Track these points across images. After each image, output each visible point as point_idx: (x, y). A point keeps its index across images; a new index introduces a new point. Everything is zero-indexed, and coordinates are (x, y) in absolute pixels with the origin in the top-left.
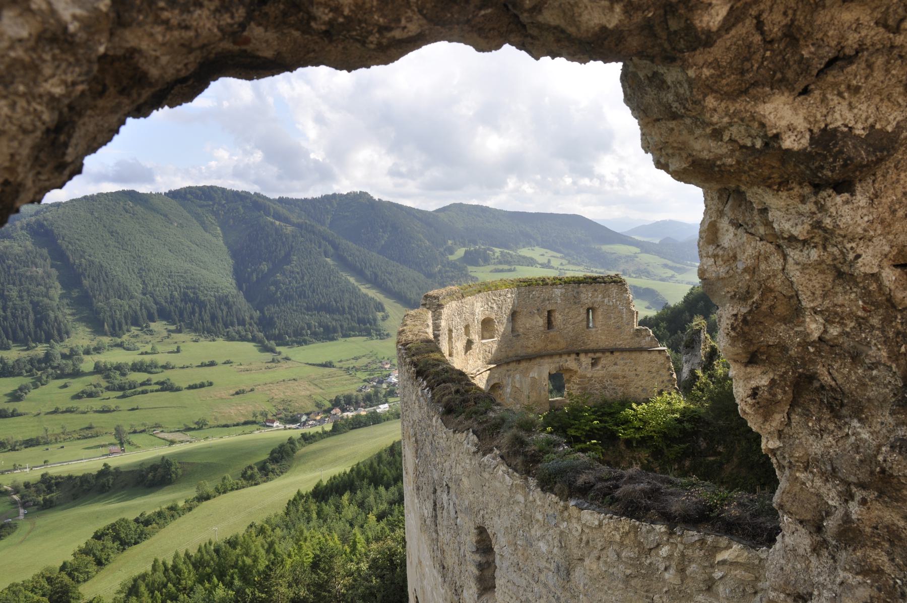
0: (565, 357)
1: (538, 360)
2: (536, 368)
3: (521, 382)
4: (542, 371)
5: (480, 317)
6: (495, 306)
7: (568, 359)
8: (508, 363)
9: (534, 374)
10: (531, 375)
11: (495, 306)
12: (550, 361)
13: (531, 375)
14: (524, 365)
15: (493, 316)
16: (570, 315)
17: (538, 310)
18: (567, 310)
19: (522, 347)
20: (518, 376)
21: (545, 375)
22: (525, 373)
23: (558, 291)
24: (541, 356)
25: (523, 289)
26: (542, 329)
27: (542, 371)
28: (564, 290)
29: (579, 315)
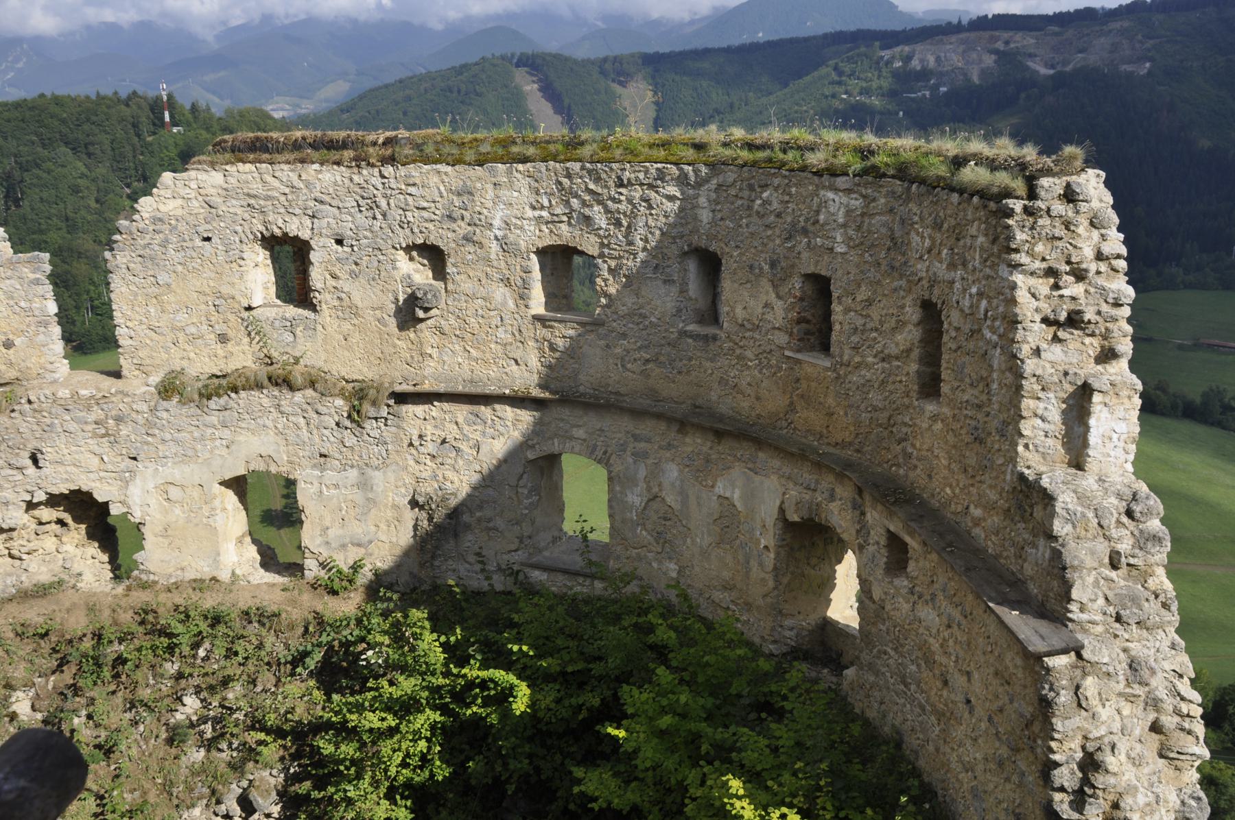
0: (827, 481)
1: (745, 450)
2: (737, 471)
3: (683, 494)
4: (762, 495)
5: (532, 236)
6: (597, 212)
7: (839, 491)
8: (638, 413)
9: (731, 486)
10: (720, 488)
11: (597, 212)
12: (786, 470)
13: (720, 488)
14: (695, 443)
15: (590, 245)
16: (875, 313)
17: (773, 265)
18: (863, 293)
19: (722, 381)
20: (672, 472)
21: (768, 511)
22: (703, 470)
23: (837, 203)
24: (759, 442)
25: (730, 176)
26: (782, 338)
27: (762, 495)
28: (857, 203)
29: (900, 325)
